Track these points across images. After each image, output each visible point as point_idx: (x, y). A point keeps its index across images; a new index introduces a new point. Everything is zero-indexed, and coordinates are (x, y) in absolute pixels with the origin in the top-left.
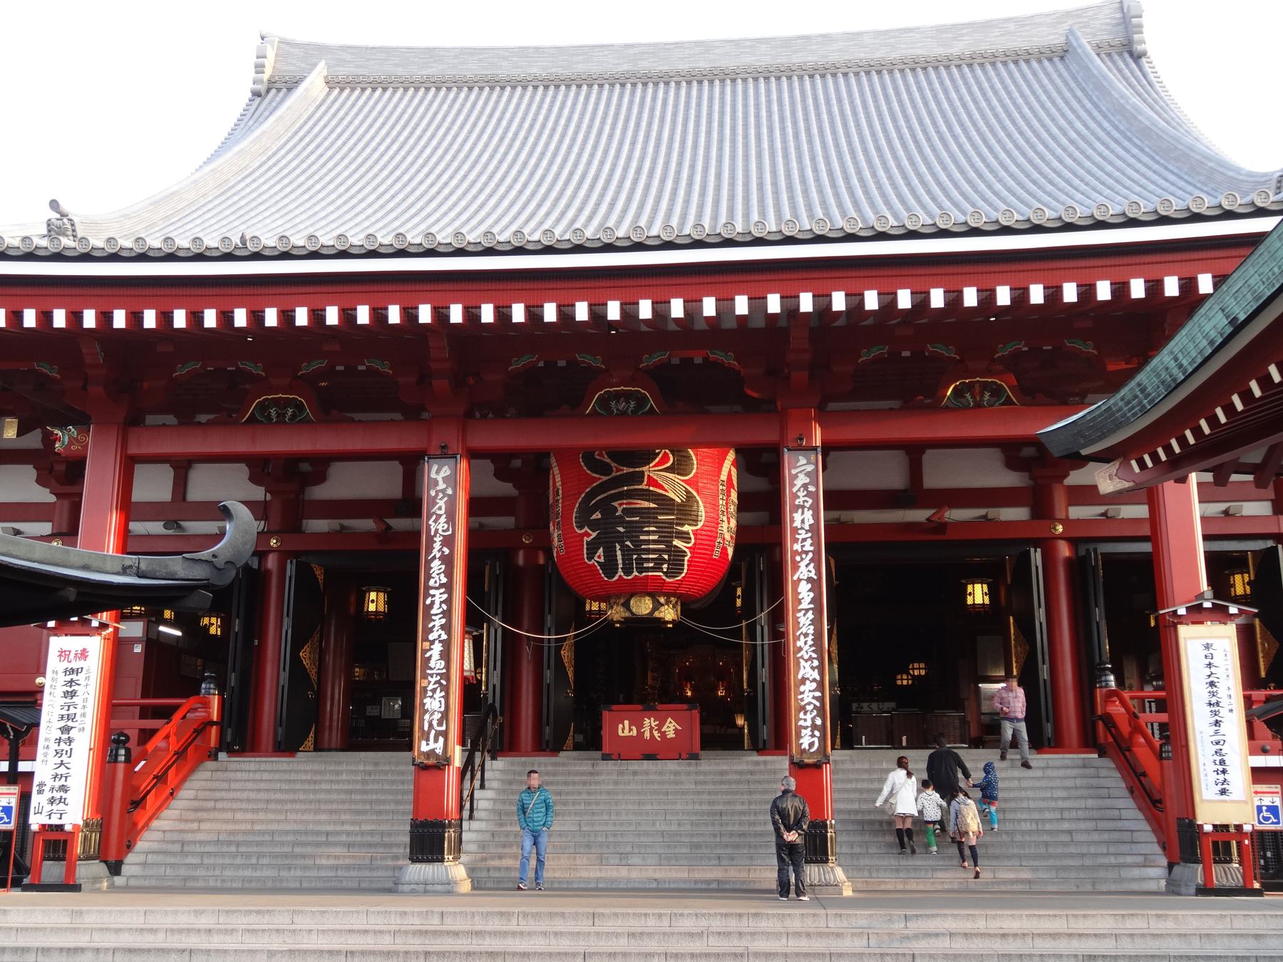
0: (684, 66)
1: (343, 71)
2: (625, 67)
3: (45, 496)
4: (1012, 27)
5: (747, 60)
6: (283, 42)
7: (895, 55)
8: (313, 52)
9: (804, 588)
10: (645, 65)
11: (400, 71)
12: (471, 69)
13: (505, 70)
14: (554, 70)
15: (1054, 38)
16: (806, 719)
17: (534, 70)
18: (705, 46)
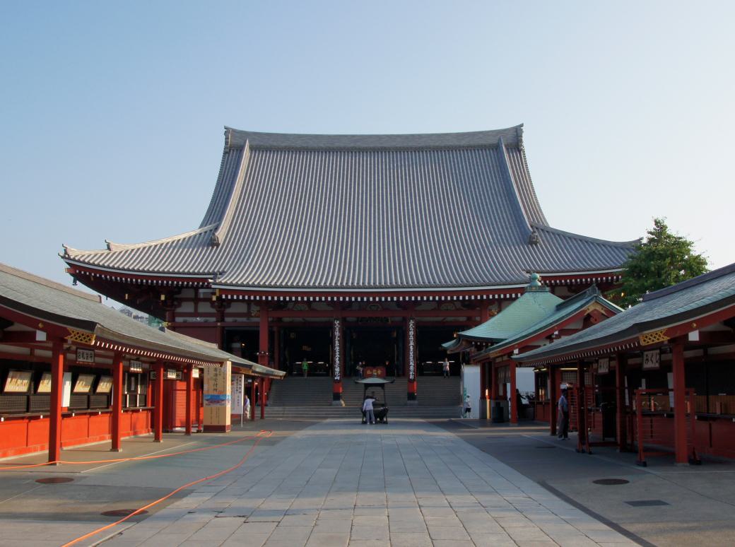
0: (372, 145)
1: (254, 143)
2: (352, 145)
3: (214, 311)
4: (481, 136)
5: (394, 144)
6: (234, 131)
7: (443, 145)
8: (245, 135)
9: (411, 347)
10: (359, 144)
11: (275, 144)
12: (299, 144)
13: (311, 144)
14: (328, 145)
15: (493, 141)
16: (411, 373)
17: (322, 145)
18: (379, 137)
